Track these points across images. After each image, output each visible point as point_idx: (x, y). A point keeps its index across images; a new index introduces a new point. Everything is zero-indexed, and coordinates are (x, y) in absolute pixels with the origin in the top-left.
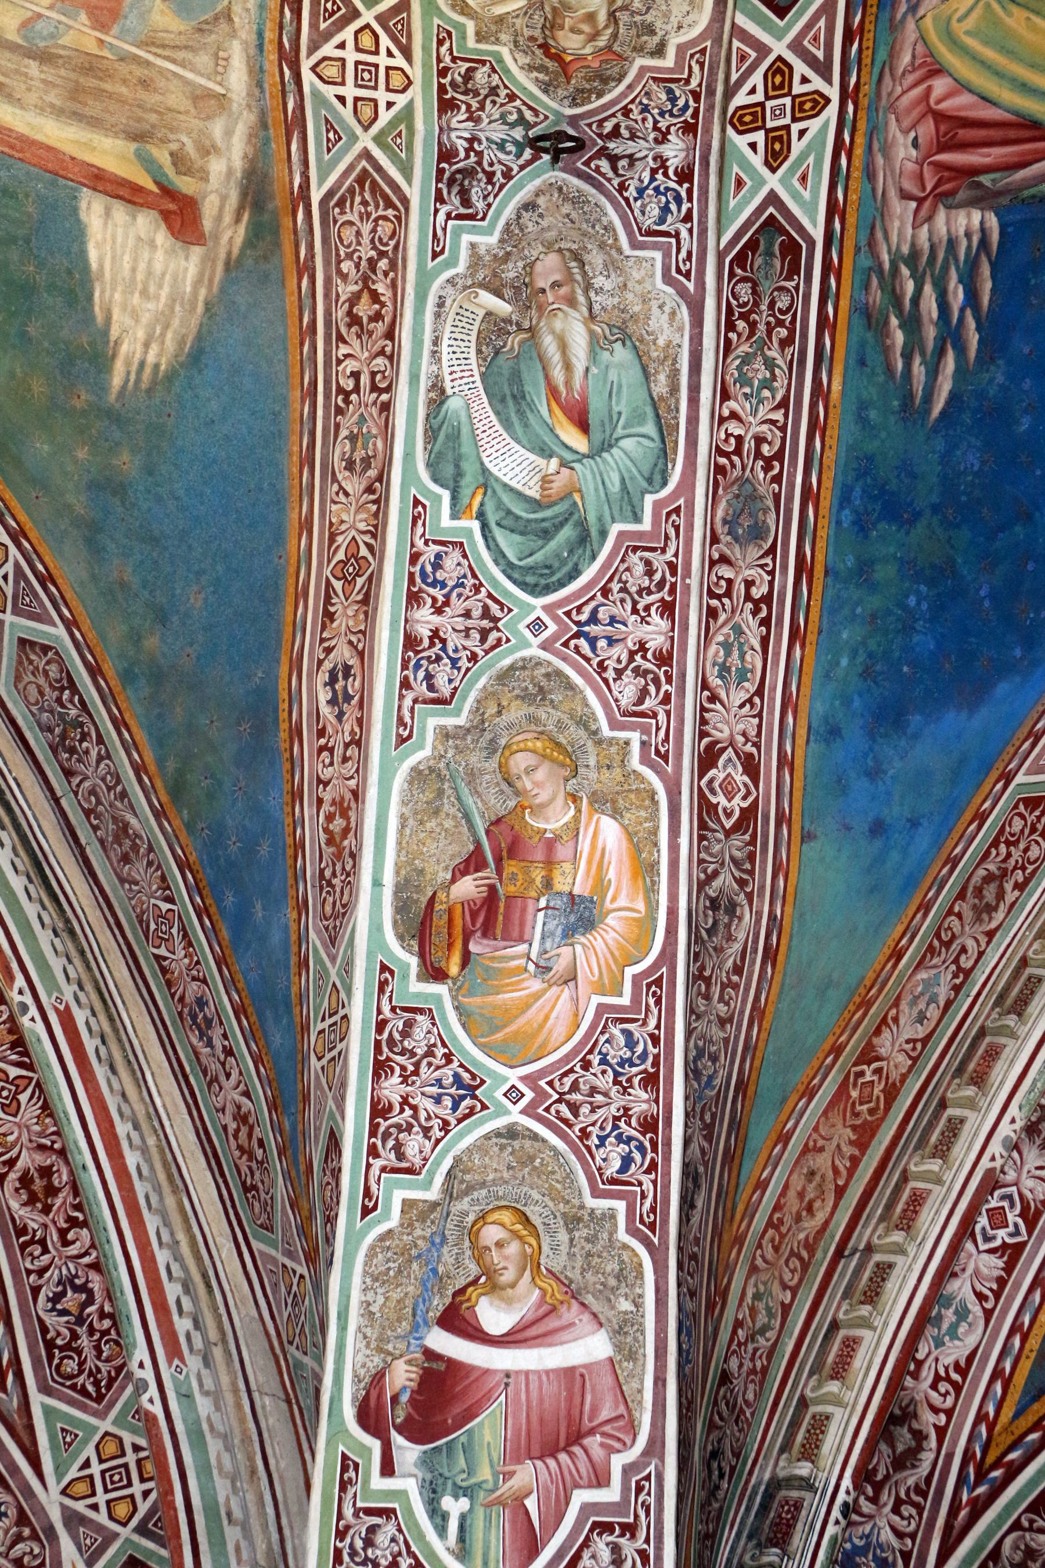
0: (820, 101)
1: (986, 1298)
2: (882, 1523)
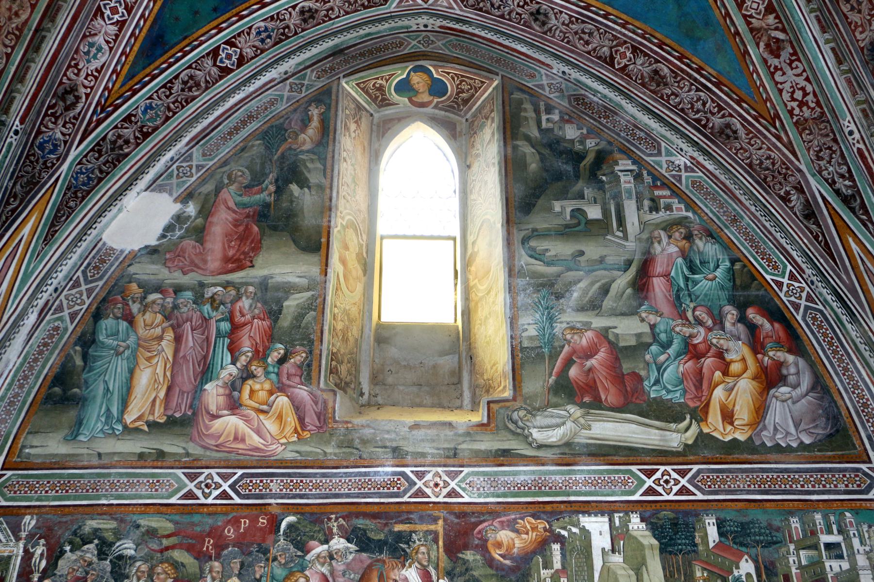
1: (110, 42)
2: (57, 131)
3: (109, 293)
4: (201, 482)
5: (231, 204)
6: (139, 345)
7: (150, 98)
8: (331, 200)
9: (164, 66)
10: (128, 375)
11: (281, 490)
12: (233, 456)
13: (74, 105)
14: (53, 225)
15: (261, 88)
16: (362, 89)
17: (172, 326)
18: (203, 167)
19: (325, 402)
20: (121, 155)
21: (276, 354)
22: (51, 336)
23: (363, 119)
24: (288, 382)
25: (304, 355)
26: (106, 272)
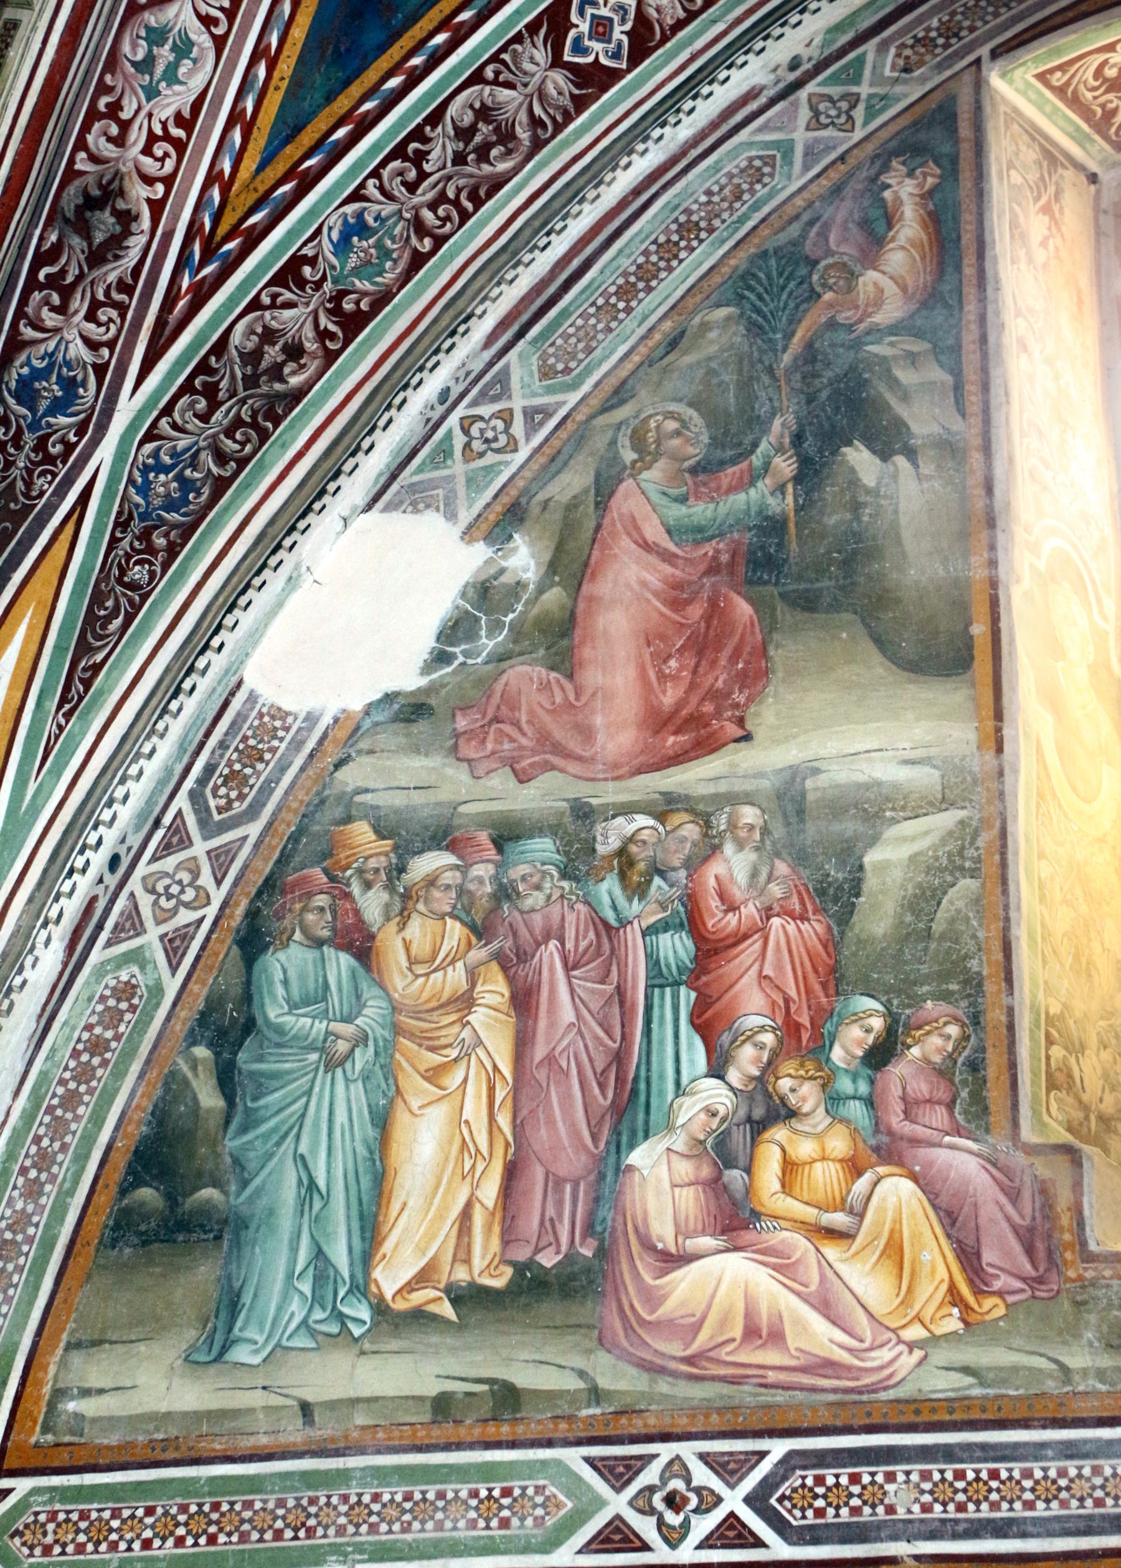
1: (215, 22)
2: (71, 334)
3: (284, 859)
4: (651, 1489)
5: (654, 532)
6: (397, 1030)
7: (356, 196)
8: (989, 489)
9: (394, 82)
10: (371, 1133)
11: (926, 1508)
12: (746, 1394)
13: (116, 244)
14: (83, 648)
15: (714, 125)
16: (1060, 91)
17: (500, 958)
18: (546, 412)
19: (1044, 1190)
20: (279, 396)
21: (855, 1032)
22: (113, 1018)
23: (1070, 198)
24: (907, 1128)
25: (953, 1030)
26: (267, 790)
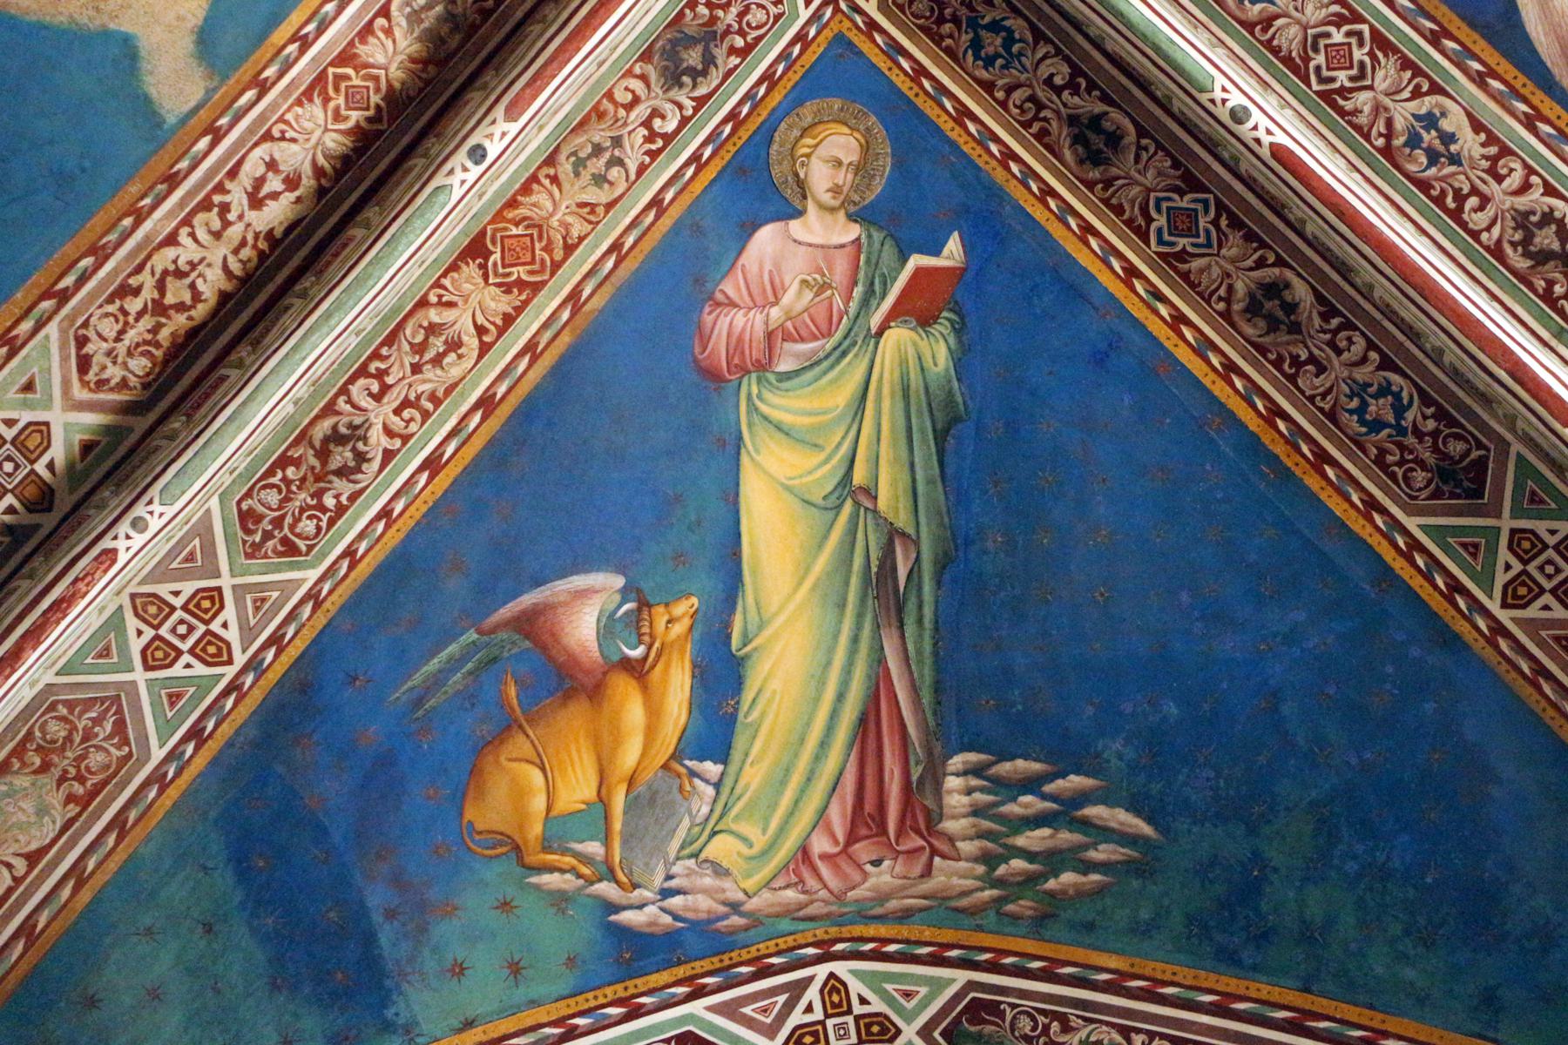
0: (834, 985)
